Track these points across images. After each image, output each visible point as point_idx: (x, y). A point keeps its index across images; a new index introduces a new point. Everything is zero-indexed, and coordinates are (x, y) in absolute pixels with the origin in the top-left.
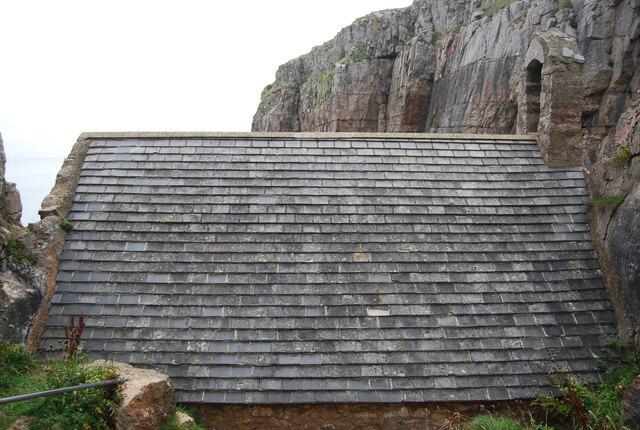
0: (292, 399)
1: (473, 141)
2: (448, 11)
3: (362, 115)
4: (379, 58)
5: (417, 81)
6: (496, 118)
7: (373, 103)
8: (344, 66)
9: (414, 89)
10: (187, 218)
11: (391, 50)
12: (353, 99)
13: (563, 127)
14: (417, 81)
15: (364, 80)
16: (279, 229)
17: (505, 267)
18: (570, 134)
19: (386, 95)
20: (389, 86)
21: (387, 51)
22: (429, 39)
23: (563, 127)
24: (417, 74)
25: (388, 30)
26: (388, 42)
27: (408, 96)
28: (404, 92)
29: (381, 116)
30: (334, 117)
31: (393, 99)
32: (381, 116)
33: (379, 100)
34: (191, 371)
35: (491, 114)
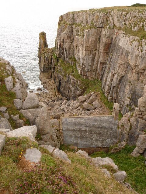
0: (87, 147)
1: (106, 116)
2: (118, 20)
3: (93, 45)
4: (98, 27)
5: (108, 39)
6: (124, 64)
7: (96, 41)
8: (87, 31)
9: (107, 42)
10: (75, 129)
11: (101, 26)
12: (90, 40)
13: (116, 116)
14: (108, 39)
15: (93, 35)
16: (84, 130)
17: (107, 134)
18: (117, 117)
19: (100, 39)
20: (100, 36)
21: (100, 26)
22: (112, 27)
23: (116, 116)
24: (108, 37)
25: (101, 20)
26: (101, 23)
27: (105, 43)
28: (104, 41)
29: (98, 45)
30: (85, 45)
31: (101, 42)
32: (98, 45)
33: (98, 40)
34: (78, 145)
35: (124, 63)
